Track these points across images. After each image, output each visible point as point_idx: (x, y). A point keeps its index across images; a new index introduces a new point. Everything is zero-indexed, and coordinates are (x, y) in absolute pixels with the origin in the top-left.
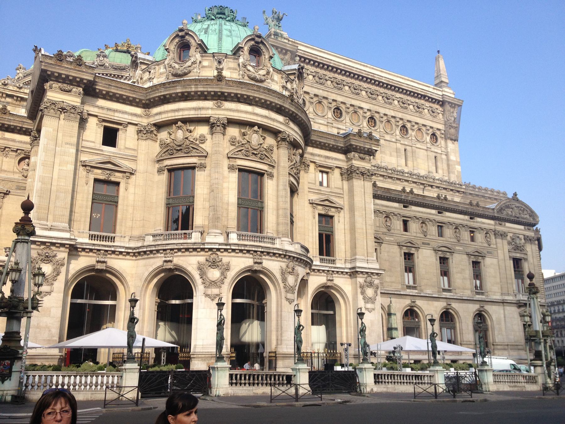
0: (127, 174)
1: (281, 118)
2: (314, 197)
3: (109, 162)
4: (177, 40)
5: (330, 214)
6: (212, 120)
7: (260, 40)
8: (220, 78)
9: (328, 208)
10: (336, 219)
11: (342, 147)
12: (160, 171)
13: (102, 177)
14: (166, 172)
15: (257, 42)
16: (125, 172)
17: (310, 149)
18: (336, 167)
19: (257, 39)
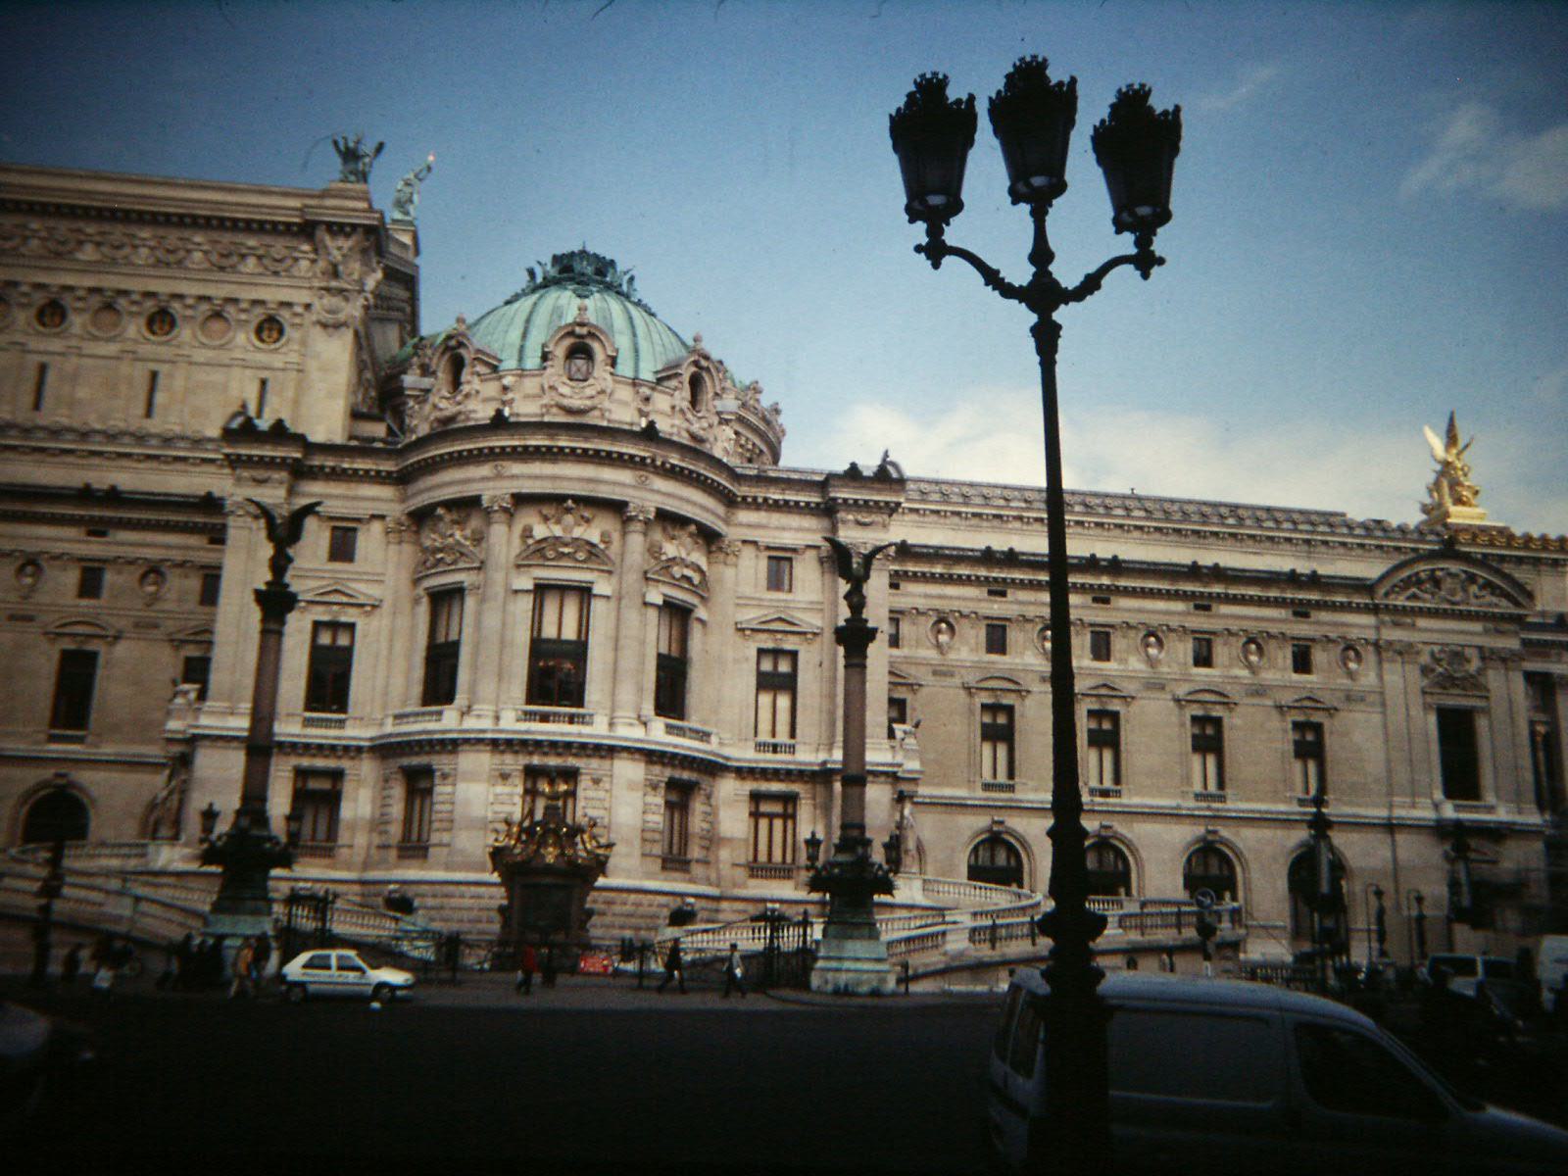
0: (368, 608)
1: (625, 476)
2: (750, 616)
3: (336, 591)
4: (447, 357)
5: (787, 646)
6: (485, 503)
7: (584, 331)
8: (499, 423)
9: (779, 636)
10: (801, 657)
11: (818, 504)
12: (416, 601)
13: (326, 618)
14: (425, 601)
15: (581, 337)
16: (362, 606)
17: (744, 516)
18: (809, 547)
19: (578, 330)
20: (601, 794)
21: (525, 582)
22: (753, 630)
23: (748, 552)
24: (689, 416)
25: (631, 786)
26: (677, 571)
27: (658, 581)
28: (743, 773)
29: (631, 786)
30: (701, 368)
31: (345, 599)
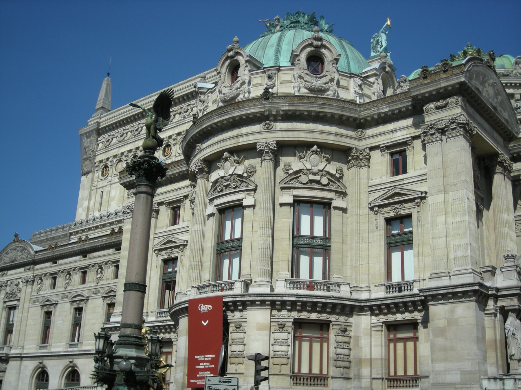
0: (181, 247)
5: (404, 212)
9: (396, 206)
15: (232, 57)
20: (241, 335)
21: (211, 209)
22: (380, 206)
23: (376, 155)
24: (307, 78)
25: (260, 328)
26: (304, 179)
27: (290, 188)
28: (376, 308)
29: (260, 328)
30: (317, 47)
31: (172, 245)
